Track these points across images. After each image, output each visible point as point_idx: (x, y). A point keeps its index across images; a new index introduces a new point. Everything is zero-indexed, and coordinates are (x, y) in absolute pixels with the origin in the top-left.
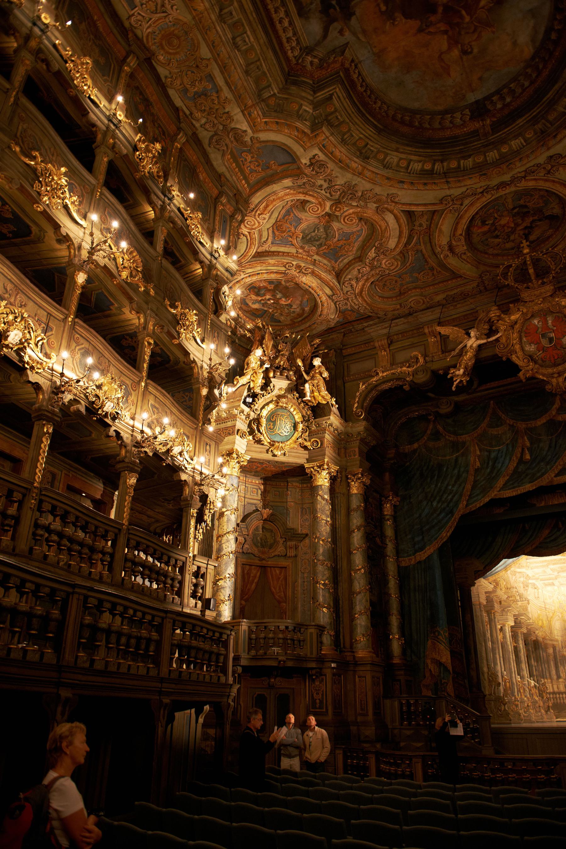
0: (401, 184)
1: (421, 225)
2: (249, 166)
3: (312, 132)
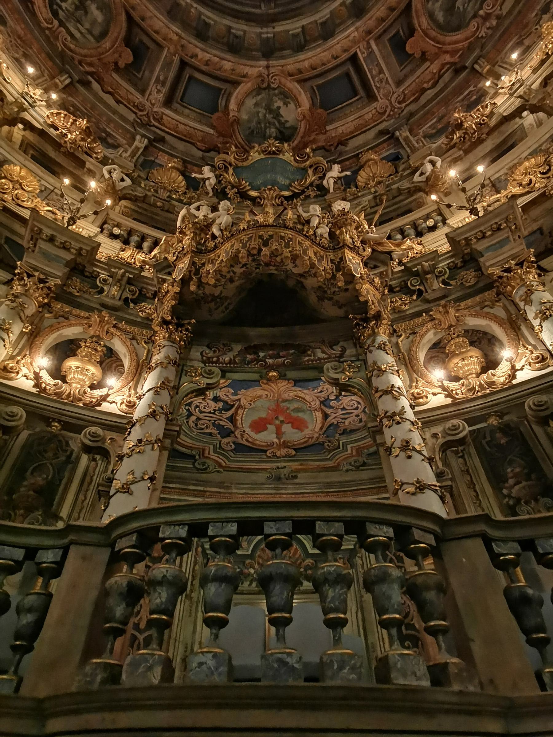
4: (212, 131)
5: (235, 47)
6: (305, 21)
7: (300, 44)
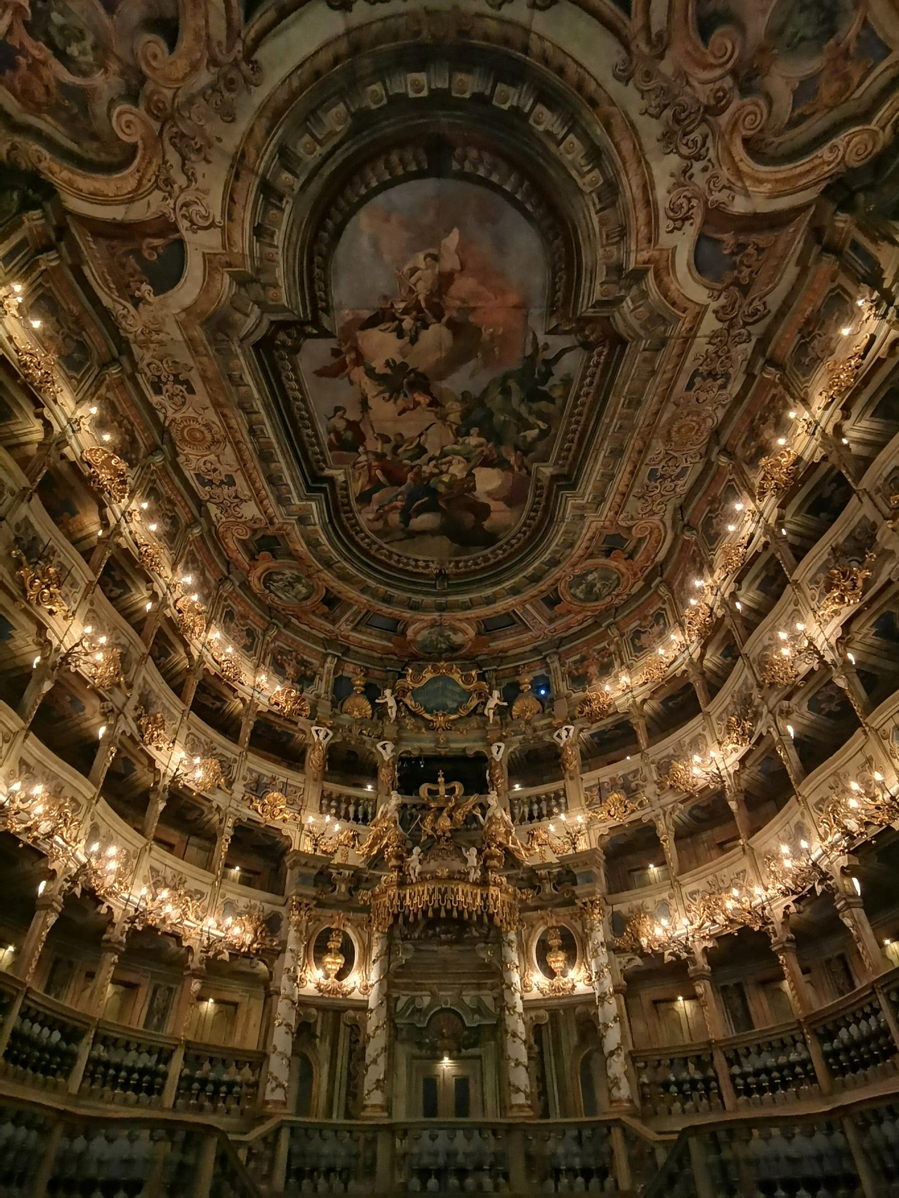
3: (646, 271)
5: (415, 607)
6: (472, 596)
7: (466, 607)
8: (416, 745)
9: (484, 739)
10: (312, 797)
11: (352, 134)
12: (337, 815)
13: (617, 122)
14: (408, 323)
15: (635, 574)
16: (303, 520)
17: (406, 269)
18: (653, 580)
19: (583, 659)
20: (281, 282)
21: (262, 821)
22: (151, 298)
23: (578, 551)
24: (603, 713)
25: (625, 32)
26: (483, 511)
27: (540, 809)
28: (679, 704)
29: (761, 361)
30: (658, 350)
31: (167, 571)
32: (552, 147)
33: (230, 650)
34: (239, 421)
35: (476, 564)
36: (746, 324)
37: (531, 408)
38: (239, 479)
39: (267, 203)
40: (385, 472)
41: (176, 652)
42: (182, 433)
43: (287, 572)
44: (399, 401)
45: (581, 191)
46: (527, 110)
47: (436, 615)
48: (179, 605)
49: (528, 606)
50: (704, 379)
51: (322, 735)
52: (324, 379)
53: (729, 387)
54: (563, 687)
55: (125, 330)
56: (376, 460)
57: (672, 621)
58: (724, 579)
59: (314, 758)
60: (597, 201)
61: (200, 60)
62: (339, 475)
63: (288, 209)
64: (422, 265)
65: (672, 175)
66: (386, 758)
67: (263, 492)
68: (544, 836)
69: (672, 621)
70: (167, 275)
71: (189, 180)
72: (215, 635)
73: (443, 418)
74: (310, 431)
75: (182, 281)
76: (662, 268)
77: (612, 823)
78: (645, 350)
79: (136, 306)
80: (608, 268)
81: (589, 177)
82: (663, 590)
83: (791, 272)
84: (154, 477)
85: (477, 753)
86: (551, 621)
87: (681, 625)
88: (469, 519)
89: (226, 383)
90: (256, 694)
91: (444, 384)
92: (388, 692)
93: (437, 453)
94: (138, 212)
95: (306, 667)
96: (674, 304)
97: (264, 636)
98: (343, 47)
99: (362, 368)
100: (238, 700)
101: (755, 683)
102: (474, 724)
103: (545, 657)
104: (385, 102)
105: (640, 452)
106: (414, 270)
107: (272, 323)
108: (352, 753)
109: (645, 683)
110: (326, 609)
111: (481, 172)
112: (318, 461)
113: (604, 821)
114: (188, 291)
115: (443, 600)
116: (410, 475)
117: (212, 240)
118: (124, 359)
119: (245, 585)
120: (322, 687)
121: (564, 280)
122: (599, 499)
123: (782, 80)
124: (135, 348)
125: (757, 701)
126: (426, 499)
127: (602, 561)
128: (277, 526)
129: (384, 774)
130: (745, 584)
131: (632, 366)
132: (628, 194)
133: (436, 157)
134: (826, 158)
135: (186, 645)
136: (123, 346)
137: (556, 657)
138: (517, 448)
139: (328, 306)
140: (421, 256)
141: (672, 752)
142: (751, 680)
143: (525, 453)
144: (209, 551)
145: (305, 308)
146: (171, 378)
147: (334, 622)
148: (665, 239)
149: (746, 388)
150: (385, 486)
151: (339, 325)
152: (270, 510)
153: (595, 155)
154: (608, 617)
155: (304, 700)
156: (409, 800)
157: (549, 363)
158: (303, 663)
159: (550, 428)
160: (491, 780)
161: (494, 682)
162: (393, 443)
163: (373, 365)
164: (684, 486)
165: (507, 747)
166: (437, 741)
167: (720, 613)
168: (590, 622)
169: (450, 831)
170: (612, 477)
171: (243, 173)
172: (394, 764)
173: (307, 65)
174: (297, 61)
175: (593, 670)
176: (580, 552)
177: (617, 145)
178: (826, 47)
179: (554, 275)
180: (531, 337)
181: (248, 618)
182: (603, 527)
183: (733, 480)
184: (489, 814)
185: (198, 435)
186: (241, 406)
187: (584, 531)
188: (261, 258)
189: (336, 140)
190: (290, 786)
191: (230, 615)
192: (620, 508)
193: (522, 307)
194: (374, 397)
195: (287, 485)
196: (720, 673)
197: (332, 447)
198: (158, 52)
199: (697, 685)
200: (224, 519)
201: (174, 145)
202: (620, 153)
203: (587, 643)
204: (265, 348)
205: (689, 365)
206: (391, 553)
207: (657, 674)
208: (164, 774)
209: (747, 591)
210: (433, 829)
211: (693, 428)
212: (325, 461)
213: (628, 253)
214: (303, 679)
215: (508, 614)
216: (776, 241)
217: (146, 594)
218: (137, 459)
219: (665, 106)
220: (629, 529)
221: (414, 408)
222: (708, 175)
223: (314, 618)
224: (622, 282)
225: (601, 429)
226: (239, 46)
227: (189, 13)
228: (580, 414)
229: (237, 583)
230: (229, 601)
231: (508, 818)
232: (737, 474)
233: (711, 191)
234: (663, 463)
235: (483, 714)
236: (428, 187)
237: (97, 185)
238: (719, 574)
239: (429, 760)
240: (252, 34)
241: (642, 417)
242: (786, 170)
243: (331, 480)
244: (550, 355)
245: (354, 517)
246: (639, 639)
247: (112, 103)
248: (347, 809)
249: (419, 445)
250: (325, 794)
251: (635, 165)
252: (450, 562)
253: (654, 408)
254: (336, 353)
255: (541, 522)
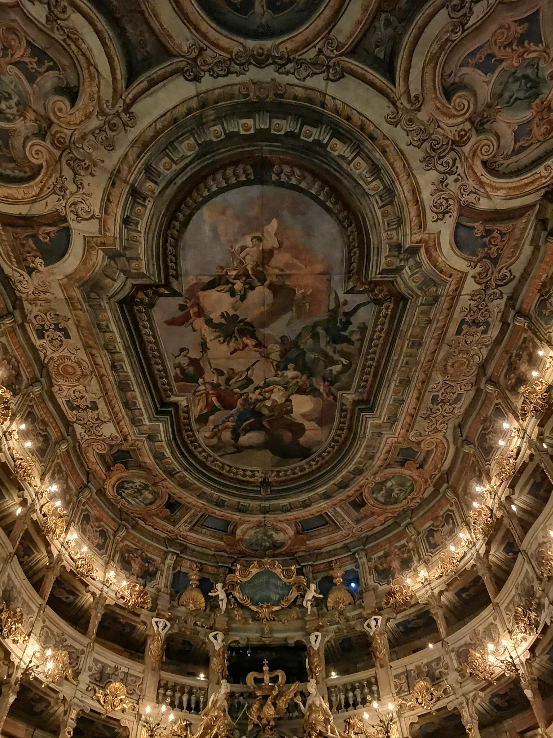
0: (375, 135)
1: (388, 23)
2: (502, 241)
3: (420, 247)
4: (222, 543)
5: (242, 510)
6: (291, 500)
8: (244, 635)
9: (303, 629)
10: (150, 687)
11: (199, 156)
12: (172, 705)
13: (391, 149)
14: (238, 286)
15: (426, 481)
16: (151, 438)
17: (237, 247)
18: (441, 486)
19: (386, 555)
20: (142, 257)
21: (103, 712)
22: (42, 268)
23: (378, 462)
24: (406, 604)
25: (392, 95)
26: (299, 430)
27: (355, 696)
28: (471, 597)
29: (512, 313)
30: (432, 305)
31: (36, 481)
32: (345, 166)
33: (85, 549)
34: (104, 359)
35: (294, 473)
36: (498, 286)
37: (335, 348)
38: (102, 405)
39: (135, 202)
40: (219, 399)
41: (39, 551)
42: (58, 369)
43: (136, 480)
44: (231, 344)
45: (367, 194)
46: (325, 142)
47: (260, 517)
48: (45, 509)
49: (338, 509)
50: (470, 326)
51: (161, 625)
52: (174, 327)
53: (490, 332)
54: (371, 580)
55: (20, 291)
56: (212, 389)
57: (459, 521)
58: (500, 485)
59: (154, 648)
60: (379, 201)
61: (91, 113)
62: (183, 402)
63: (149, 207)
64: (250, 244)
65: (433, 184)
66: (217, 648)
67: (120, 415)
68: (360, 724)
69: (459, 521)
70: (55, 252)
71: (78, 187)
72: (73, 536)
73: (266, 357)
74: (160, 367)
75: (67, 256)
76: (432, 246)
77: (421, 711)
78: (422, 304)
79: (30, 274)
80: (390, 246)
81: (372, 185)
82: (450, 494)
83: (527, 250)
84: (33, 403)
85: (298, 642)
86: (358, 521)
87: (468, 525)
88: (287, 436)
89: (95, 330)
90: (105, 589)
91: (267, 331)
92: (219, 586)
93: (262, 384)
94: (39, 209)
95: (149, 563)
96: (442, 271)
97: (114, 536)
98: (194, 104)
99: (202, 319)
100: (89, 595)
101: (535, 577)
102: (294, 615)
103: (354, 554)
104: (223, 137)
105: (423, 382)
106: (243, 248)
107: (134, 285)
108: (186, 642)
109: (441, 576)
110: (168, 512)
111: (294, 181)
112: (165, 390)
113: (412, 709)
114: (71, 262)
115: (267, 504)
116: (240, 401)
117: (92, 227)
118: (17, 313)
119: (101, 492)
120: (162, 581)
121: (357, 255)
122: (393, 419)
123: (506, 123)
124: (27, 306)
125: (539, 594)
126: (252, 420)
127: (397, 470)
128: (130, 442)
129: (216, 664)
130: (517, 489)
131: (413, 316)
132: (402, 196)
133: (261, 172)
134: (543, 174)
135: (48, 545)
136: (17, 302)
137: (363, 554)
138: (325, 379)
139: (177, 273)
140: (249, 238)
141: (469, 640)
142: (531, 574)
143: (332, 383)
144: (73, 464)
145: (159, 276)
146: (53, 326)
147: (174, 524)
148: (432, 227)
149: (503, 332)
150: (219, 410)
151: (185, 287)
152: (125, 430)
153: (376, 170)
154: (405, 519)
155: (146, 594)
156: (237, 688)
157: (348, 315)
158: (147, 560)
159: (350, 364)
160: (310, 669)
161: (311, 576)
162: (227, 375)
163: (211, 316)
164: (460, 409)
165: (324, 636)
166: (262, 631)
167: (499, 514)
168: (390, 522)
169: (274, 719)
170: (402, 402)
171: (118, 182)
172: (224, 653)
173: (168, 114)
174: (162, 112)
175: (396, 564)
176: (380, 463)
177: (391, 164)
178: (534, 104)
179: (350, 251)
180: (333, 296)
181: (101, 520)
182: (397, 442)
183: (500, 403)
184: (309, 702)
185: (70, 370)
186: (106, 347)
187: (382, 446)
188: (127, 240)
189: (187, 161)
190: (132, 676)
191: (86, 518)
192: (410, 427)
193: (327, 274)
194: (211, 341)
195: (140, 409)
196: (504, 567)
197: (177, 379)
198: (63, 107)
199: (486, 579)
200: (87, 437)
201: (69, 165)
202: (394, 169)
203: (390, 541)
204: (127, 304)
205: (457, 316)
206: (223, 464)
207: (450, 568)
208: (18, 667)
209: (520, 495)
210: (259, 717)
211: (463, 364)
212: (171, 390)
213: (405, 236)
214: (147, 575)
215: (321, 515)
216: (513, 229)
217: (17, 500)
218: (20, 389)
219: (425, 140)
220: (419, 443)
221: (243, 349)
222: (459, 184)
223: (157, 520)
224: (402, 256)
225: (391, 364)
226: (121, 103)
227: (87, 84)
228: (375, 353)
229: (94, 491)
230: (87, 506)
231: (326, 706)
232: (502, 398)
233: (462, 195)
234: (442, 391)
235: (302, 606)
236: (255, 191)
237: (10, 191)
238: (495, 481)
239: (254, 649)
240: (130, 96)
241: (423, 355)
242: (514, 182)
243: (176, 405)
244: (348, 309)
245: (194, 435)
246: (433, 536)
247: (27, 138)
248: (181, 698)
249: (247, 378)
250: (162, 683)
251: (405, 177)
252: (272, 472)
253: (432, 349)
254: (182, 307)
255: (346, 439)
